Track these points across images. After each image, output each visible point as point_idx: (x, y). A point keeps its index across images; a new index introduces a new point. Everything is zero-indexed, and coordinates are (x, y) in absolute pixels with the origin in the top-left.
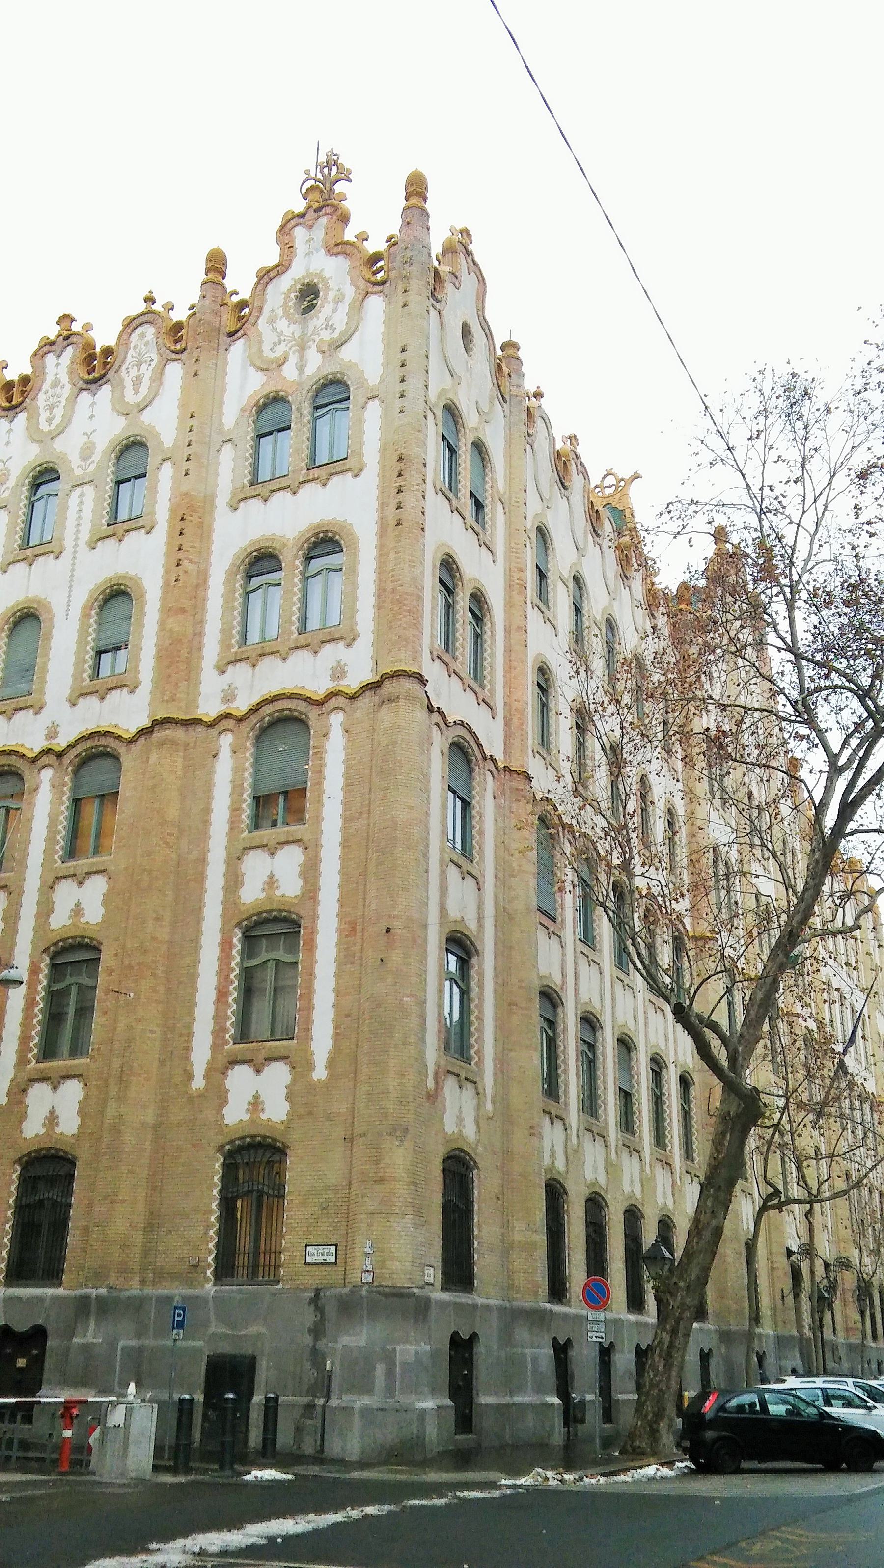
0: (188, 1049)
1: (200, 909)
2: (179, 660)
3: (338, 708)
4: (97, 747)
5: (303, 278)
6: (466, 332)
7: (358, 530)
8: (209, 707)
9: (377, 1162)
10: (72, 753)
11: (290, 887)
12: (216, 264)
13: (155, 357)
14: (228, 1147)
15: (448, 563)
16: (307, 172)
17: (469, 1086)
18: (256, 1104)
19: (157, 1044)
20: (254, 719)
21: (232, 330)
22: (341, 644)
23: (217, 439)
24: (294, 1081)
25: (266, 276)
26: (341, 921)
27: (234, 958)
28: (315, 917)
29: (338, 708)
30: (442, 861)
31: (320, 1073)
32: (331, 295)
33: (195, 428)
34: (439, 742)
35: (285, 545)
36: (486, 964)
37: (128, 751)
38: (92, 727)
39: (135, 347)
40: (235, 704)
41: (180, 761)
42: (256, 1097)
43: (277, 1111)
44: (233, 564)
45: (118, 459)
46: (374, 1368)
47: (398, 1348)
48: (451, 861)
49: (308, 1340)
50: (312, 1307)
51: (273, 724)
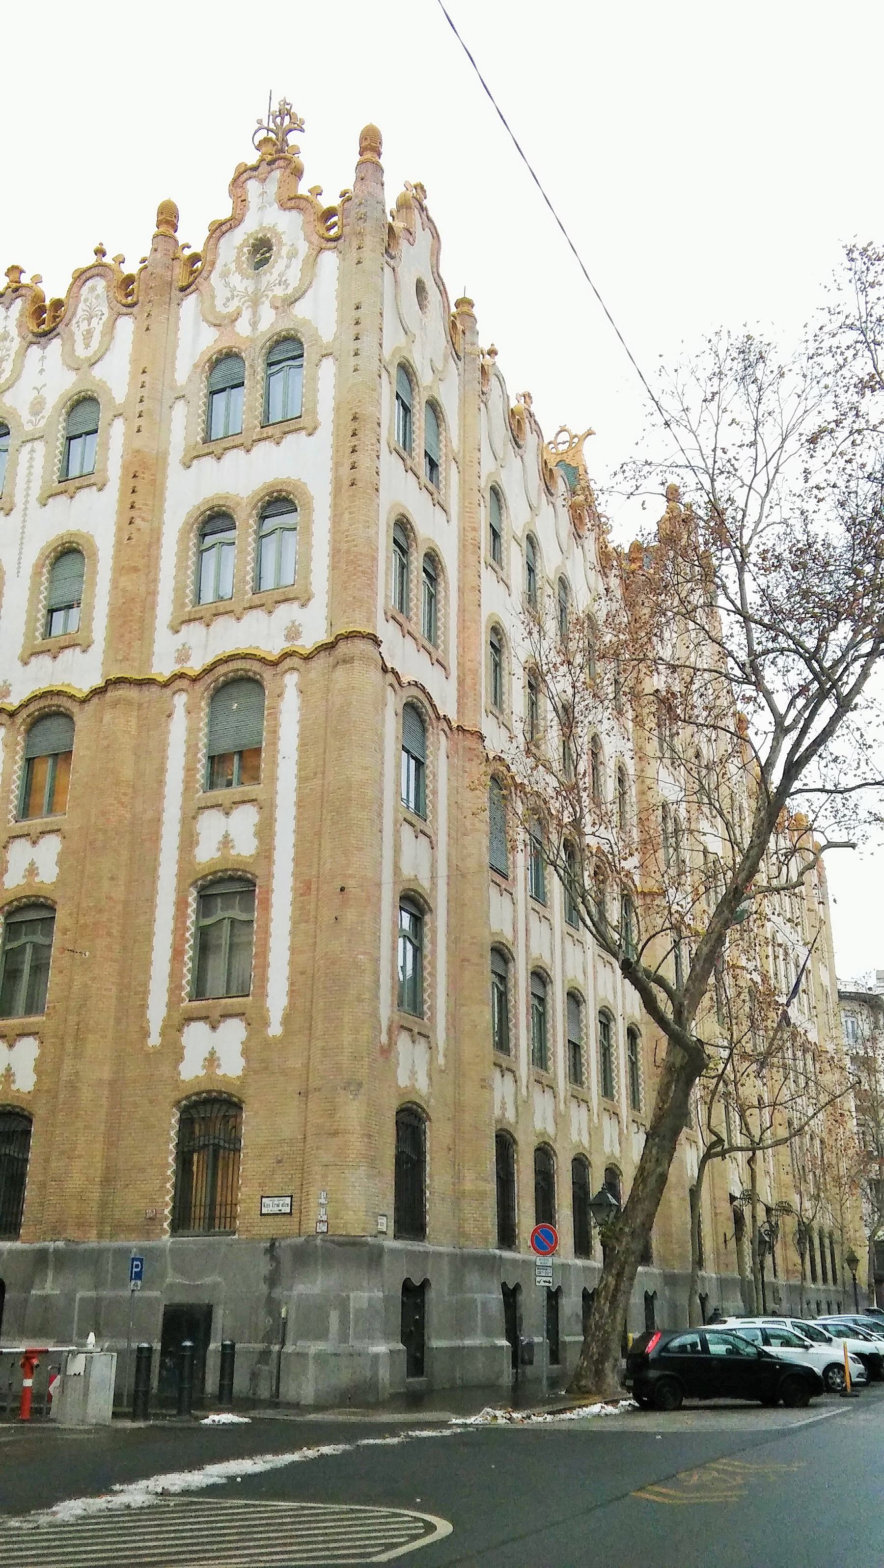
0: (144, 1007)
1: (155, 869)
2: (132, 619)
3: (293, 669)
4: (50, 706)
5: (257, 232)
6: (420, 288)
7: (312, 490)
8: (162, 667)
9: (331, 1116)
10: (24, 714)
11: (245, 847)
12: (168, 217)
13: (106, 310)
14: (184, 1102)
15: (403, 523)
16: (260, 122)
17: (422, 1040)
18: (212, 1060)
19: (114, 1001)
20: (208, 679)
21: (184, 284)
22: (296, 605)
23: (169, 396)
24: (249, 1039)
25: (219, 230)
26: (295, 880)
27: (189, 917)
28: (270, 876)
29: (293, 669)
30: (396, 821)
31: (275, 1029)
32: (284, 251)
33: (147, 384)
34: (394, 703)
35: (238, 504)
36: (439, 921)
37: (81, 710)
38: (44, 686)
39: (86, 300)
40: (189, 664)
41: (133, 722)
42: (212, 1053)
43: (232, 1067)
44: (186, 523)
45: (69, 414)
46: (328, 1316)
47: (352, 1295)
48: (405, 820)
49: (264, 1288)
50: (268, 1257)
51: (227, 684)
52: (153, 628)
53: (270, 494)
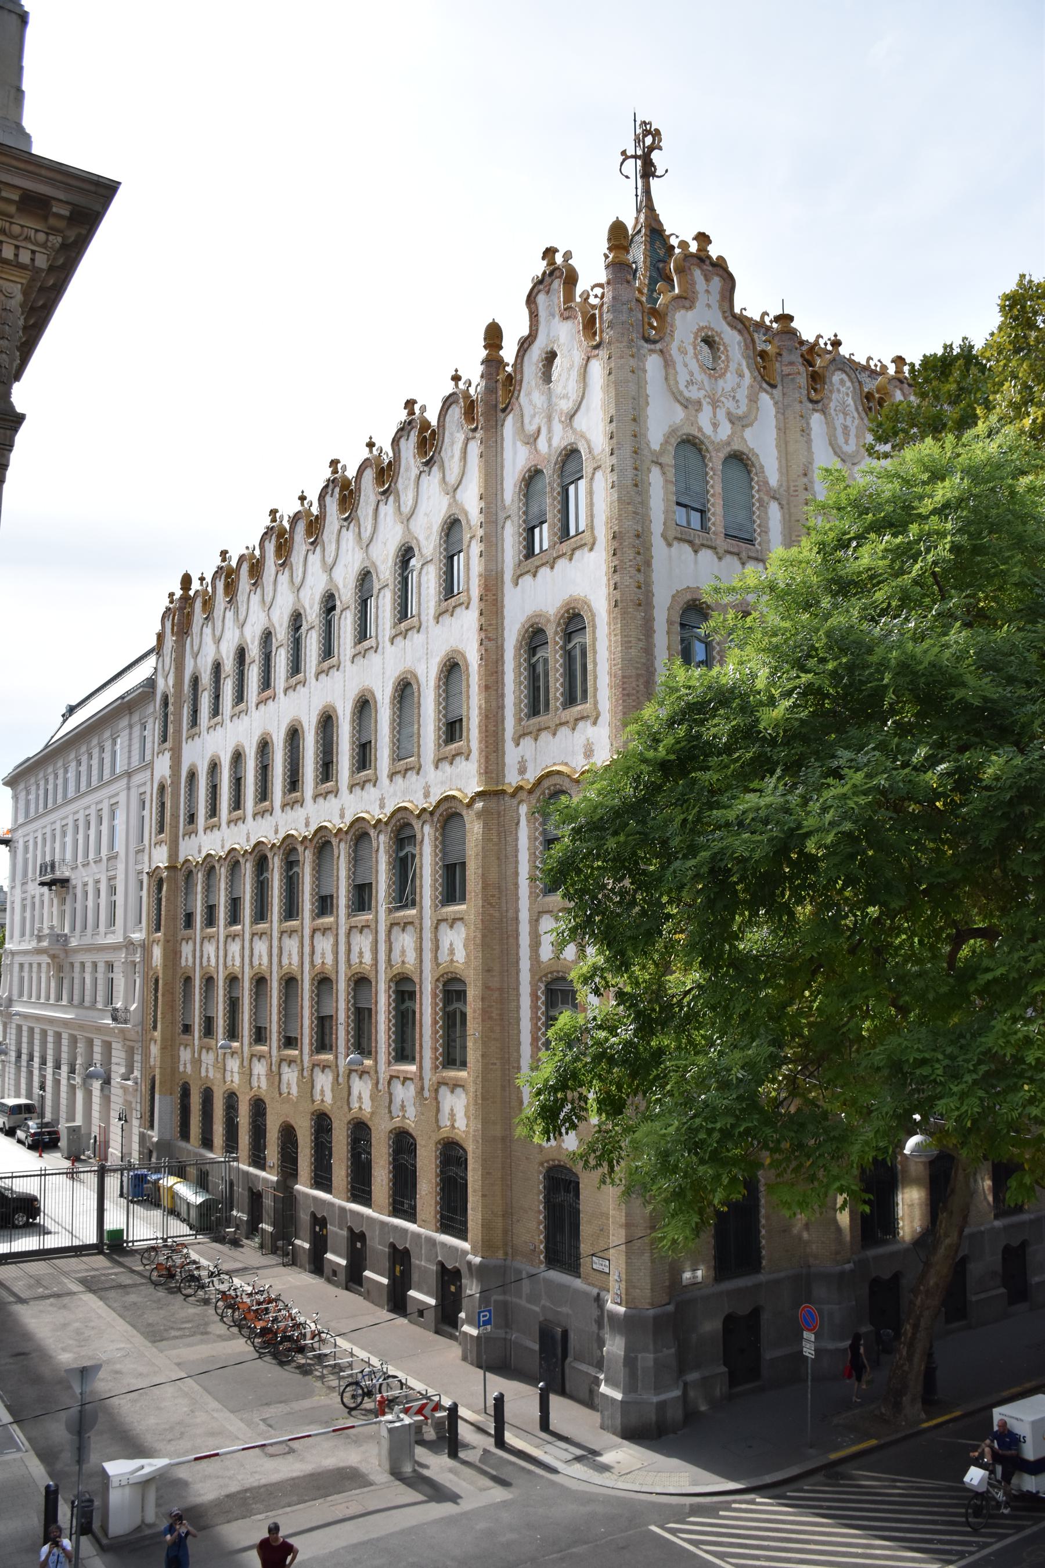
8: (512, 779)
52: (503, 740)
53: (567, 611)
